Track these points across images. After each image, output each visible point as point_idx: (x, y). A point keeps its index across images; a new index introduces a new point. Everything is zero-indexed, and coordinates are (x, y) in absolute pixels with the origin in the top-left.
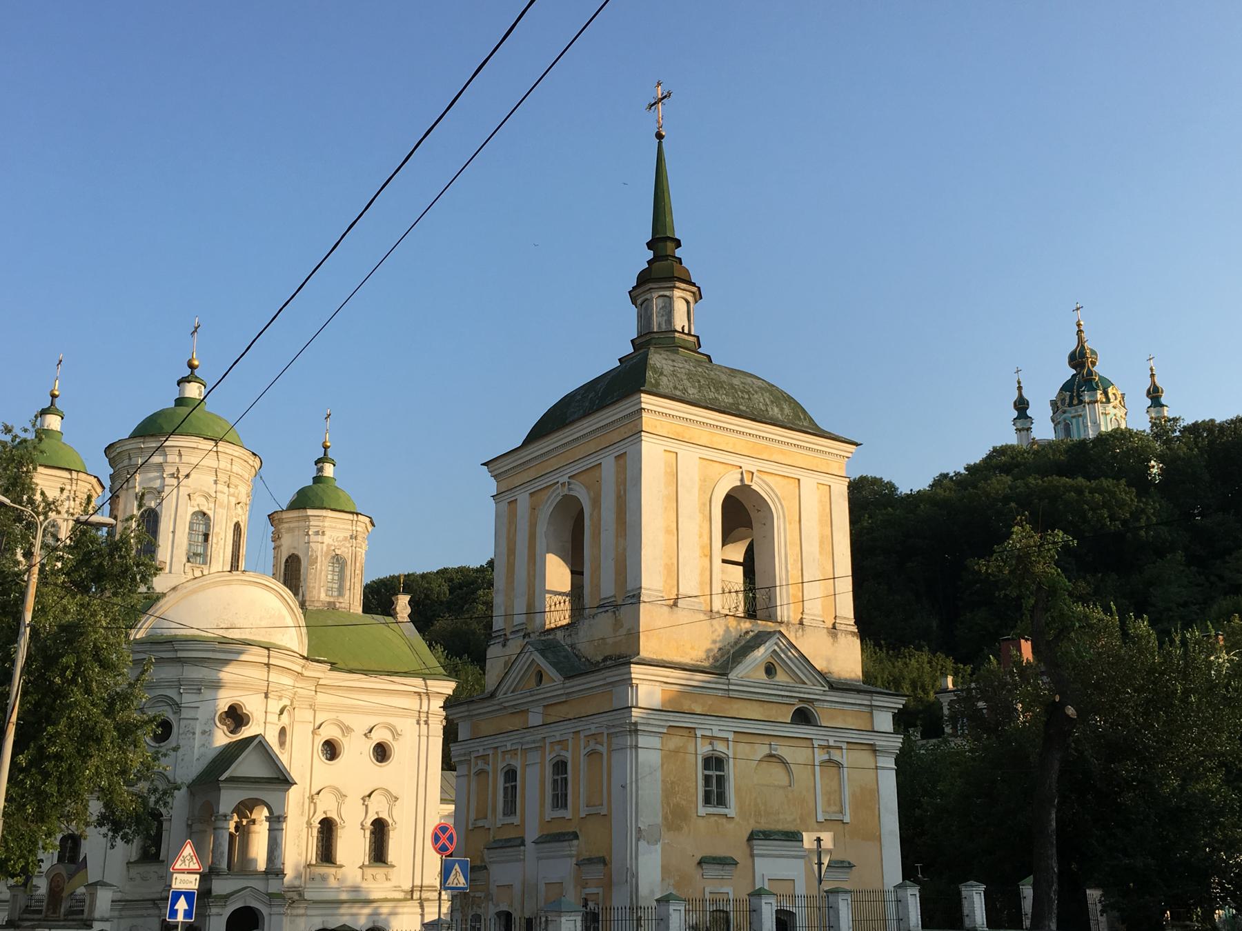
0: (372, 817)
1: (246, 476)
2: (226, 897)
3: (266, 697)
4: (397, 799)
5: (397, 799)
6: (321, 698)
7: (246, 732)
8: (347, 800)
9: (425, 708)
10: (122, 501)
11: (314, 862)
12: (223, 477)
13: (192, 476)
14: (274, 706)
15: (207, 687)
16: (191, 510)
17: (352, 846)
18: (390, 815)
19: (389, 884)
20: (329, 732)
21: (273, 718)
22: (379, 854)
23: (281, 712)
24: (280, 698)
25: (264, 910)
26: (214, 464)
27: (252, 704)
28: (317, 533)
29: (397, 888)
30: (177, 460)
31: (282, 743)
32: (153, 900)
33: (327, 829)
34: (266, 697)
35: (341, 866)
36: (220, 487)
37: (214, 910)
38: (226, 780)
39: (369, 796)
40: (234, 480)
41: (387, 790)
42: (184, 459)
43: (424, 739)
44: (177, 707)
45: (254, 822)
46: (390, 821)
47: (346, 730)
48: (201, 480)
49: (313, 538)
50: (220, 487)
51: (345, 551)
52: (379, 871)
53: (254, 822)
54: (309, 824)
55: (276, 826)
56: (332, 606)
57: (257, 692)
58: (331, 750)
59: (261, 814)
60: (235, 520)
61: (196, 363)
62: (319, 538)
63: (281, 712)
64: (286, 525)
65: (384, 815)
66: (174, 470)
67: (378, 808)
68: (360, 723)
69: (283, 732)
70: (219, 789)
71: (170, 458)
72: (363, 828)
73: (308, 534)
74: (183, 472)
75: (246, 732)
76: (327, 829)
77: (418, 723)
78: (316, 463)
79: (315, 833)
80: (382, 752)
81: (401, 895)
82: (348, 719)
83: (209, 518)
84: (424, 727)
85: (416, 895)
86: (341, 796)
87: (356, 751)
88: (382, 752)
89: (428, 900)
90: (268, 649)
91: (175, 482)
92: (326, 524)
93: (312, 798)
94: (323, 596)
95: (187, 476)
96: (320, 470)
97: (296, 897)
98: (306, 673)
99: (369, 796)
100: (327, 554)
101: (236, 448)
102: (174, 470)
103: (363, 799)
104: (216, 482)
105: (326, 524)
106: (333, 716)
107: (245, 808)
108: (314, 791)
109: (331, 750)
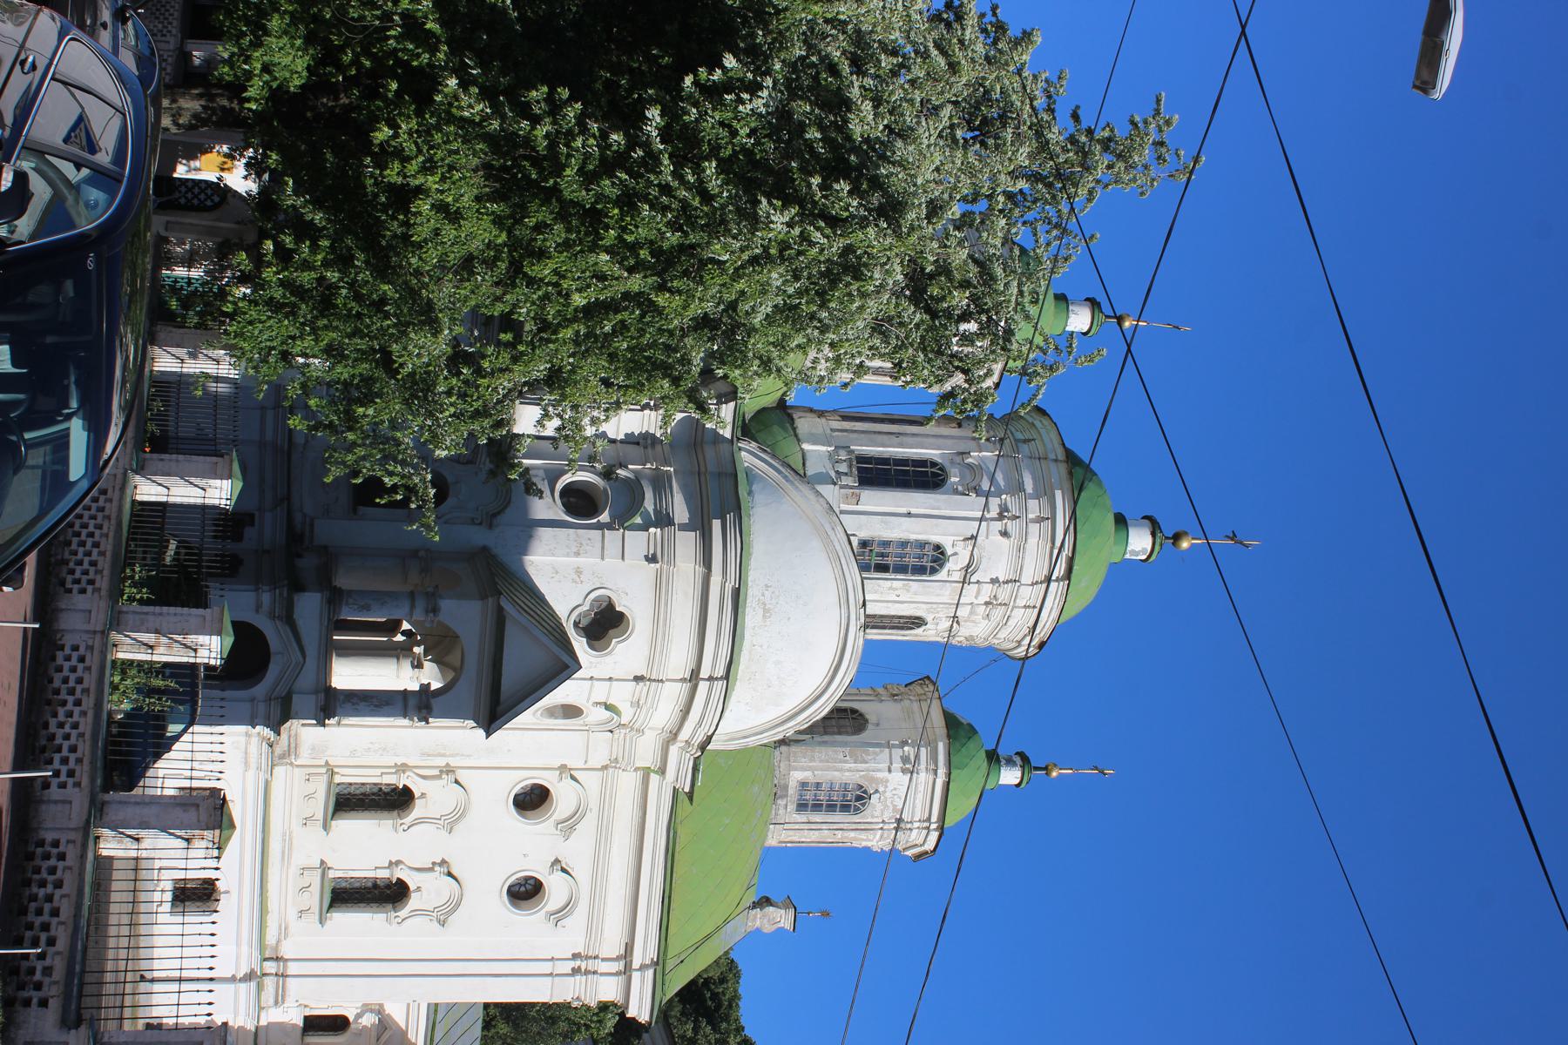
0: (412, 880)
1: (1002, 635)
2: (289, 620)
3: (638, 679)
4: (443, 923)
5: (443, 923)
6: (628, 783)
7: (579, 644)
8: (444, 833)
9: (604, 967)
10: (956, 432)
11: (338, 779)
12: (1004, 593)
13: (1004, 540)
14: (622, 695)
15: (659, 576)
16: (947, 543)
17: (365, 846)
19: (292, 914)
20: (564, 797)
21: (601, 692)
22: (347, 895)
23: (608, 707)
24: (637, 704)
25: (260, 690)
26: (1027, 578)
27: (626, 654)
28: (905, 759)
29: (284, 931)
30: (1031, 516)
31: (551, 712)
32: (288, 498)
33: (396, 800)
34: (638, 679)
36: (987, 590)
37: (266, 598)
38: (500, 610)
39: (450, 874)
40: (998, 613)
41: (458, 905)
42: (1034, 528)
43: (546, 968)
44: (621, 520)
45: (418, 665)
46: (403, 913)
47: (568, 825)
48: (997, 555)
49: (897, 753)
50: (987, 590)
51: (879, 810)
52: (314, 898)
53: (419, 666)
54: (402, 768)
55: (412, 702)
56: (778, 793)
57: (651, 662)
58: (532, 800)
59: (432, 676)
60: (929, 618)
61: (1185, 545)
62: (897, 765)
63: (608, 707)
64: (916, 705)
65: (414, 902)
66: (1014, 511)
67: (427, 891)
68: (578, 851)
69: (571, 711)
70: (483, 597)
71: (1033, 504)
72: (393, 864)
73: (904, 743)
74: (1011, 526)
75: (579, 644)
76: (396, 800)
77: (575, 956)
78: (1021, 755)
79: (390, 780)
80: (525, 892)
81: (271, 939)
82: (587, 827)
83: (934, 571)
84: (567, 967)
85: (270, 967)
86: (451, 822)
88: (525, 892)
89: (260, 988)
90: (727, 677)
91: (994, 513)
92: (923, 775)
93: (448, 770)
94: (797, 776)
95: (1005, 534)
96: (1014, 764)
97: (278, 750)
99: (450, 874)
100: (872, 780)
101: (1055, 614)
102: (1014, 511)
103: (443, 862)
104: (994, 581)
105: (923, 775)
106: (594, 804)
107: (441, 646)
108: (462, 775)
109: (532, 800)
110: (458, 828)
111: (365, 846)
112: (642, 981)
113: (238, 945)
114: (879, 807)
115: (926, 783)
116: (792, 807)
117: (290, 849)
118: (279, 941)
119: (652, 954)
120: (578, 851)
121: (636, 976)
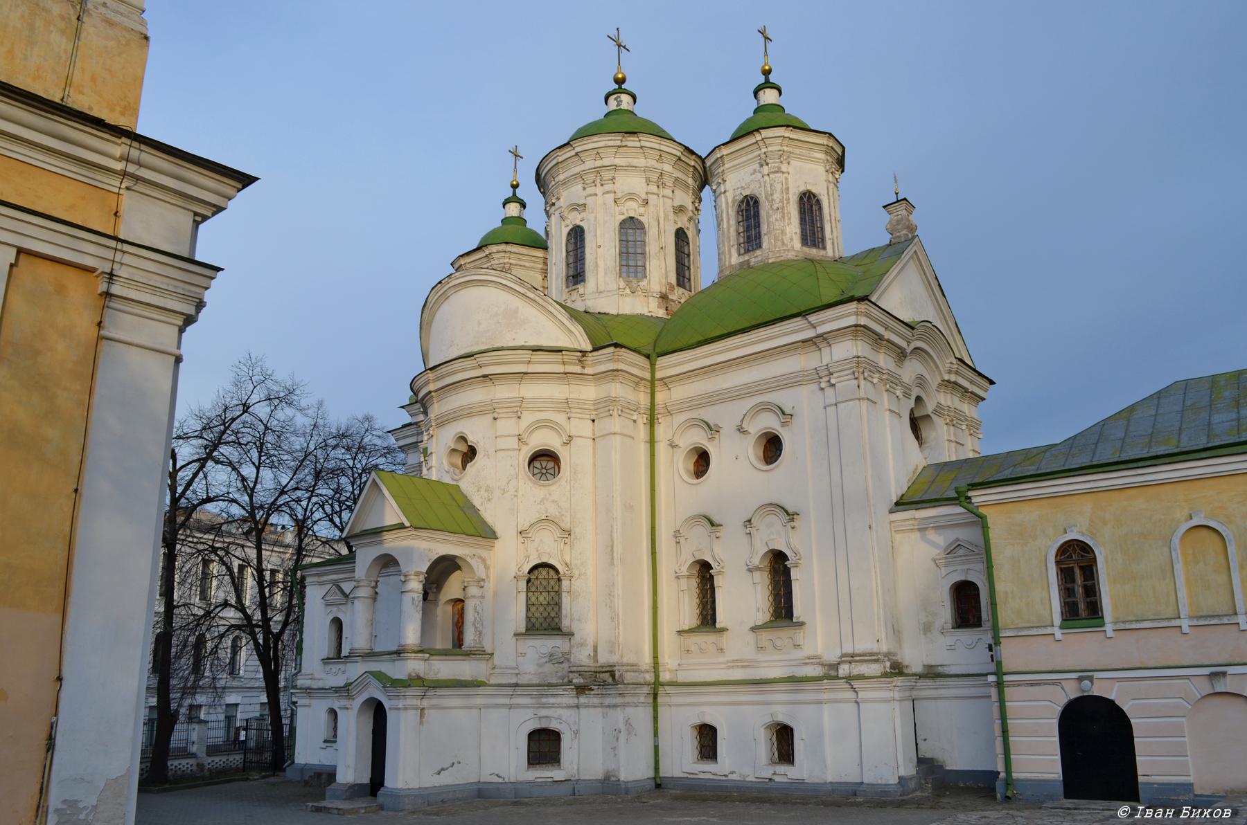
5: (791, 516)
16: (565, 231)
18: (789, 546)
35: (723, 630)
47: (712, 429)
56: (746, 266)
67: (774, 536)
80: (772, 447)
81: (816, 671)
82: (709, 414)
84: (829, 391)
87: (734, 459)
89: (861, 677)
98: (588, 370)
100: (734, 202)
101: (595, 138)
110: (715, 519)
111: (742, 598)
112: (823, 323)
113: (820, 702)
114: (752, 186)
115: (733, 160)
116: (758, 252)
117: (741, 661)
118: (822, 665)
119: (797, 323)
120: (726, 416)
121: (820, 330)
